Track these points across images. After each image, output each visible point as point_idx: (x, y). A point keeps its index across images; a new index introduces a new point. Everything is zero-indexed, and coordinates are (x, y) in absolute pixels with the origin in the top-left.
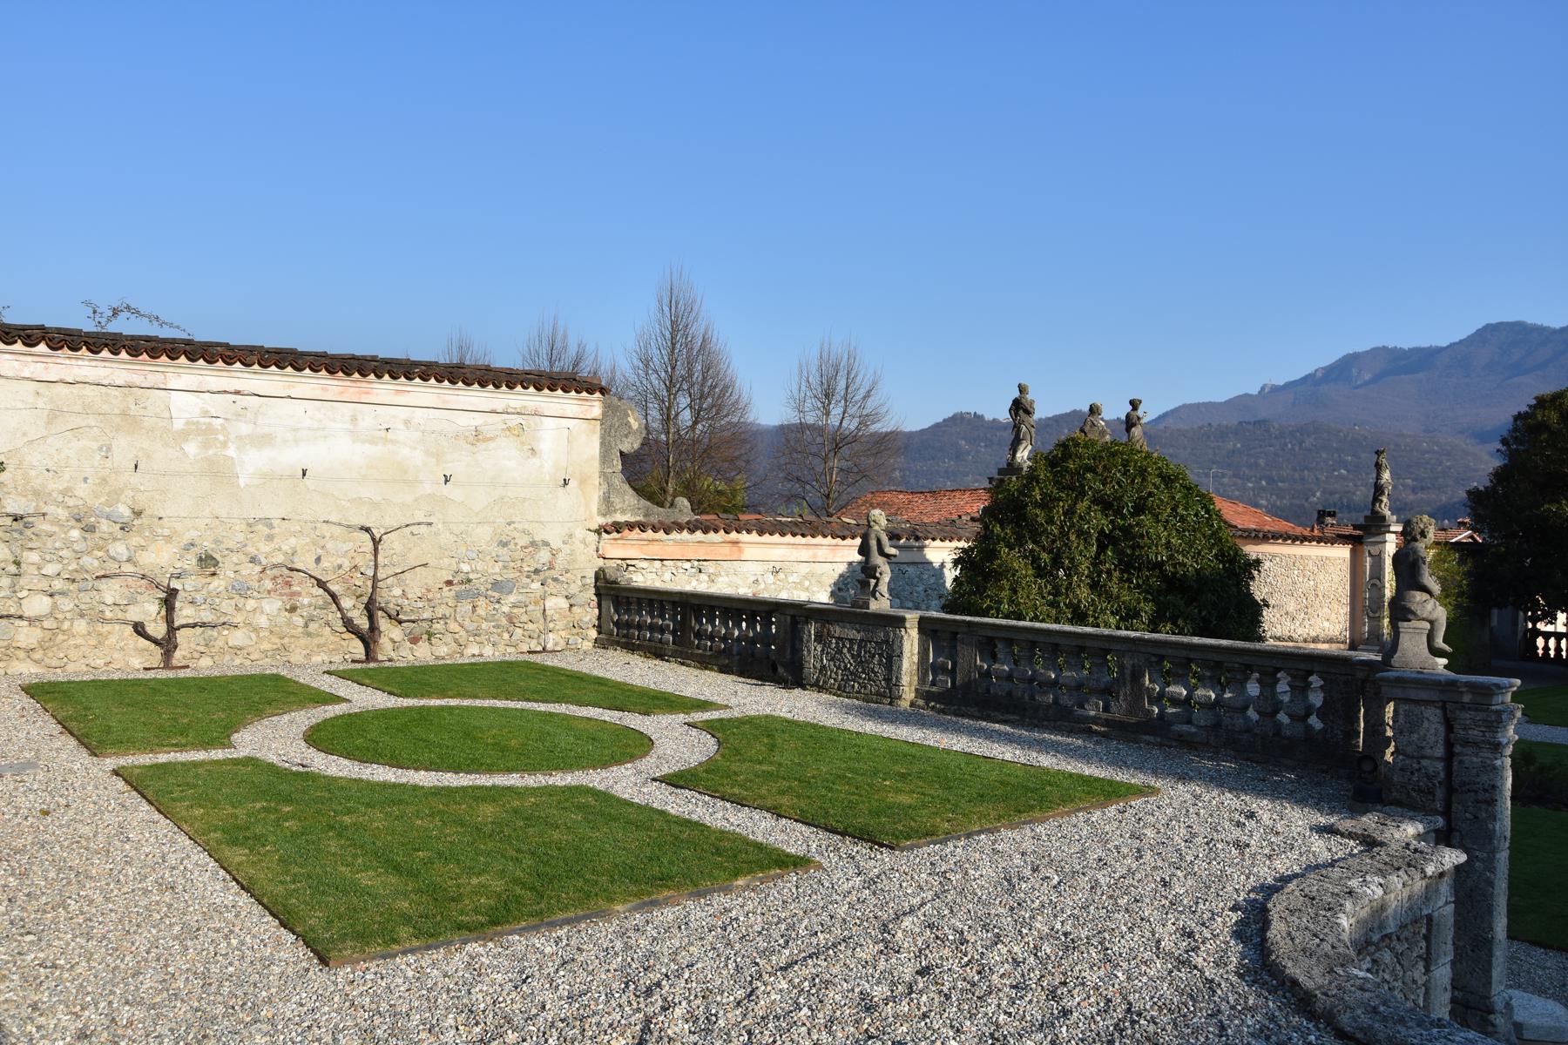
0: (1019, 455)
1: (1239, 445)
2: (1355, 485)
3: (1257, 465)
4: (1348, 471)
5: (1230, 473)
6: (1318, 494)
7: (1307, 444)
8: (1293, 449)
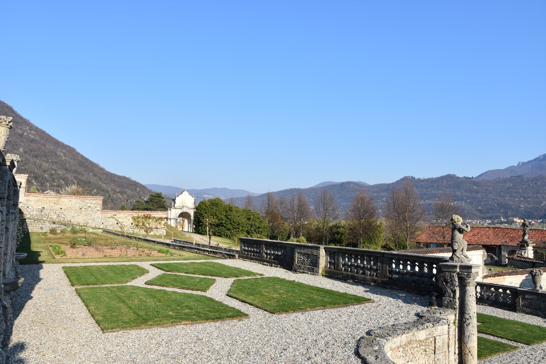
0: (525, 238)
1: (511, 185)
3: (519, 192)
5: (509, 195)
6: (544, 202)
8: (532, 186)
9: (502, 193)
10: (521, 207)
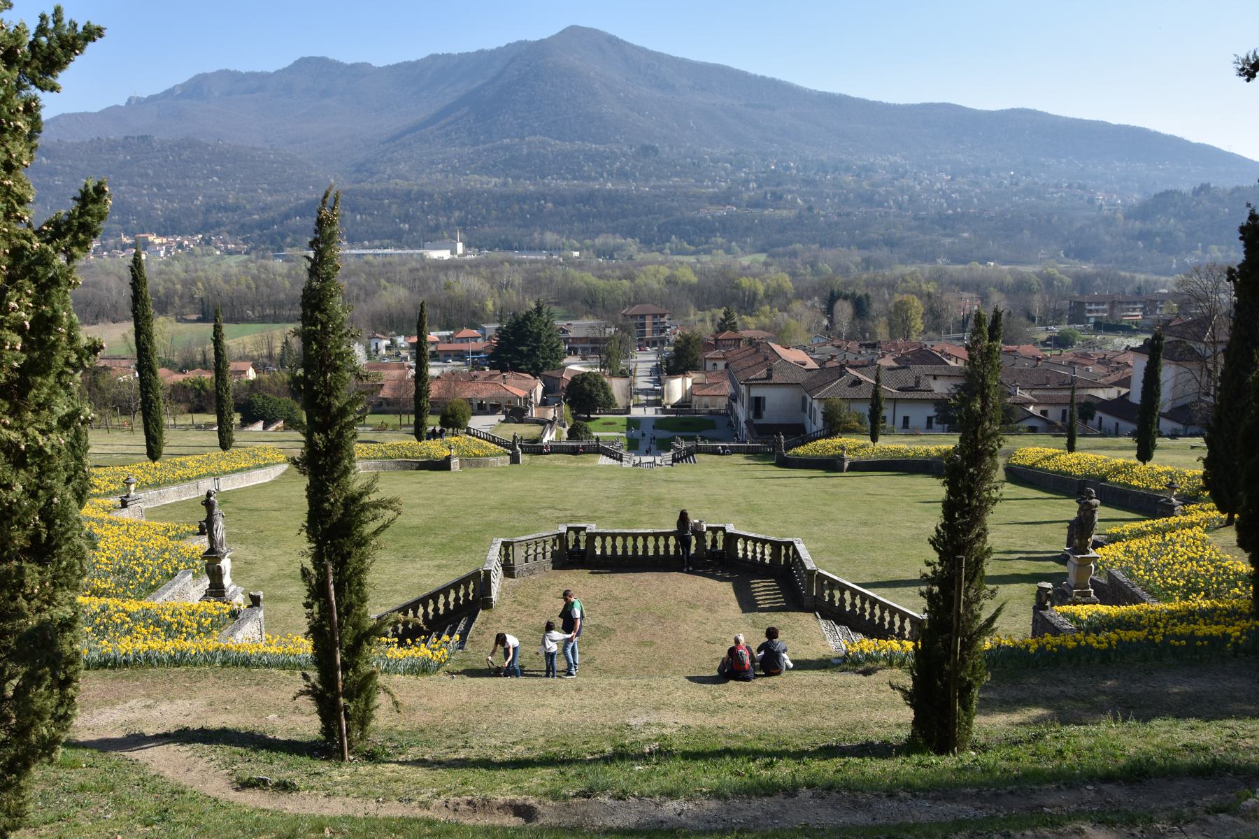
1: (129, 158)
3: (147, 175)
4: (219, 178)
6: (200, 198)
7: (184, 157)
10: (157, 209)
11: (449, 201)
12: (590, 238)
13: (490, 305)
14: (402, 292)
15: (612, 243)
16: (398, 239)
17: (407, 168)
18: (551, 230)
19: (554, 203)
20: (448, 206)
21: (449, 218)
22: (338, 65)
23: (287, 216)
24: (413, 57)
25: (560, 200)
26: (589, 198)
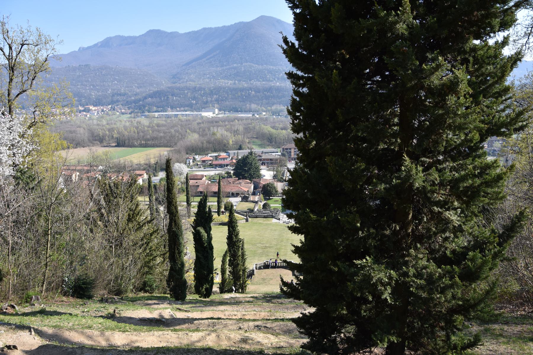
2: (121, 87)
3: (88, 81)
5: (80, 84)
6: (110, 90)
7: (103, 73)
8: (99, 75)
9: (74, 81)
10: (92, 95)
11: (212, 91)
12: (270, 107)
13: (231, 142)
14: (196, 136)
15: (279, 108)
16: (191, 107)
17: (194, 77)
18: (254, 103)
19: (255, 92)
20: (211, 93)
21: (212, 98)
22: (165, 33)
23: (145, 98)
24: (196, 29)
25: (257, 90)
26: (270, 89)
